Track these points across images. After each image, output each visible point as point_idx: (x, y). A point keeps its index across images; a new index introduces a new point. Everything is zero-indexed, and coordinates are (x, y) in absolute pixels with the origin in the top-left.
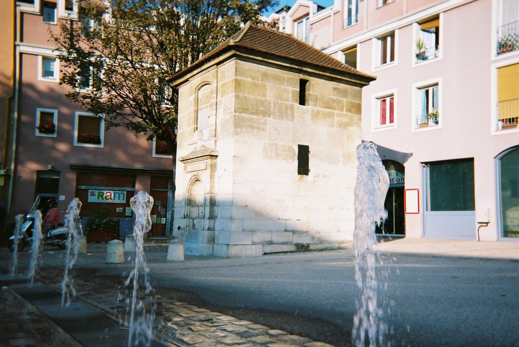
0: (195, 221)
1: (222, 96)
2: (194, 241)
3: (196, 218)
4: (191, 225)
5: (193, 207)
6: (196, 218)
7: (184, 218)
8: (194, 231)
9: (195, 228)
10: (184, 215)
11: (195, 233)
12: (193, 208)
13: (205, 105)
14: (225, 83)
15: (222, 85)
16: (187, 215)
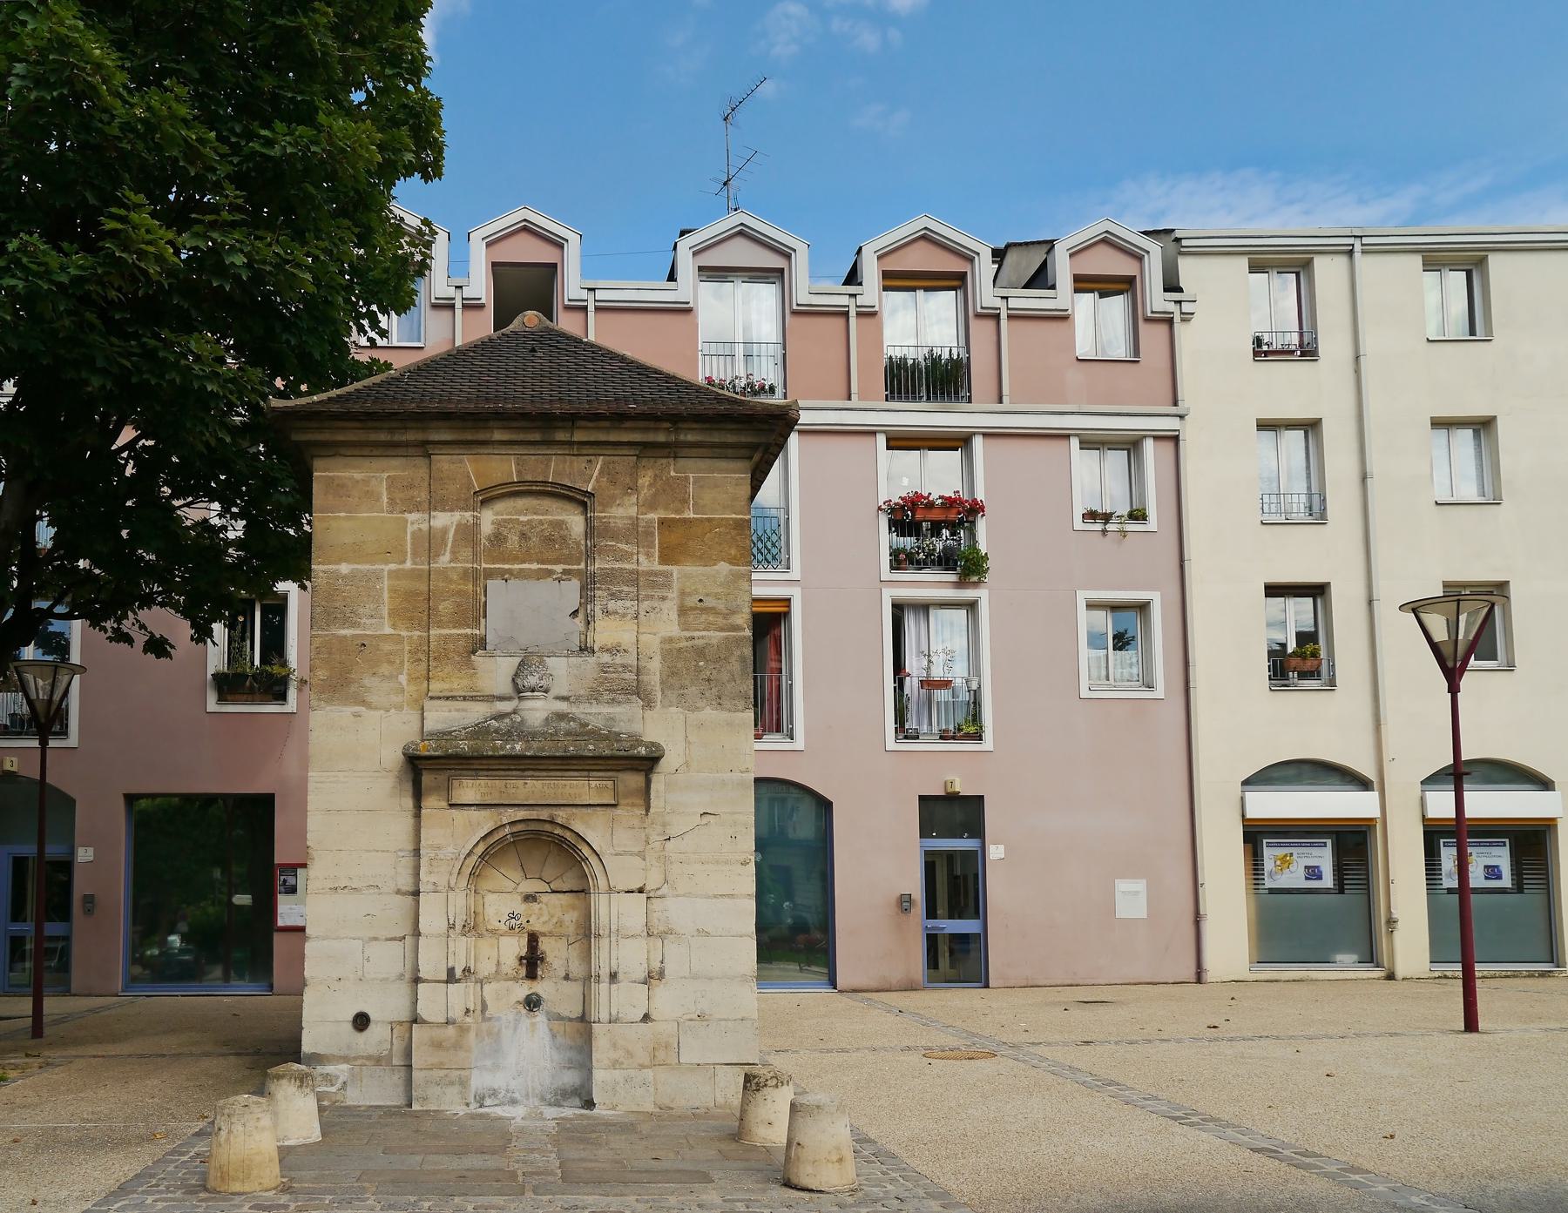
0: (486, 987)
1: (665, 559)
2: (488, 1063)
3: (488, 979)
4: (479, 1008)
5: (481, 936)
6: (488, 979)
7: (451, 977)
8: (485, 1026)
9: (487, 1014)
10: (451, 972)
11: (489, 1034)
12: (481, 942)
13: (535, 566)
14: (685, 521)
15: (662, 522)
16: (467, 970)
